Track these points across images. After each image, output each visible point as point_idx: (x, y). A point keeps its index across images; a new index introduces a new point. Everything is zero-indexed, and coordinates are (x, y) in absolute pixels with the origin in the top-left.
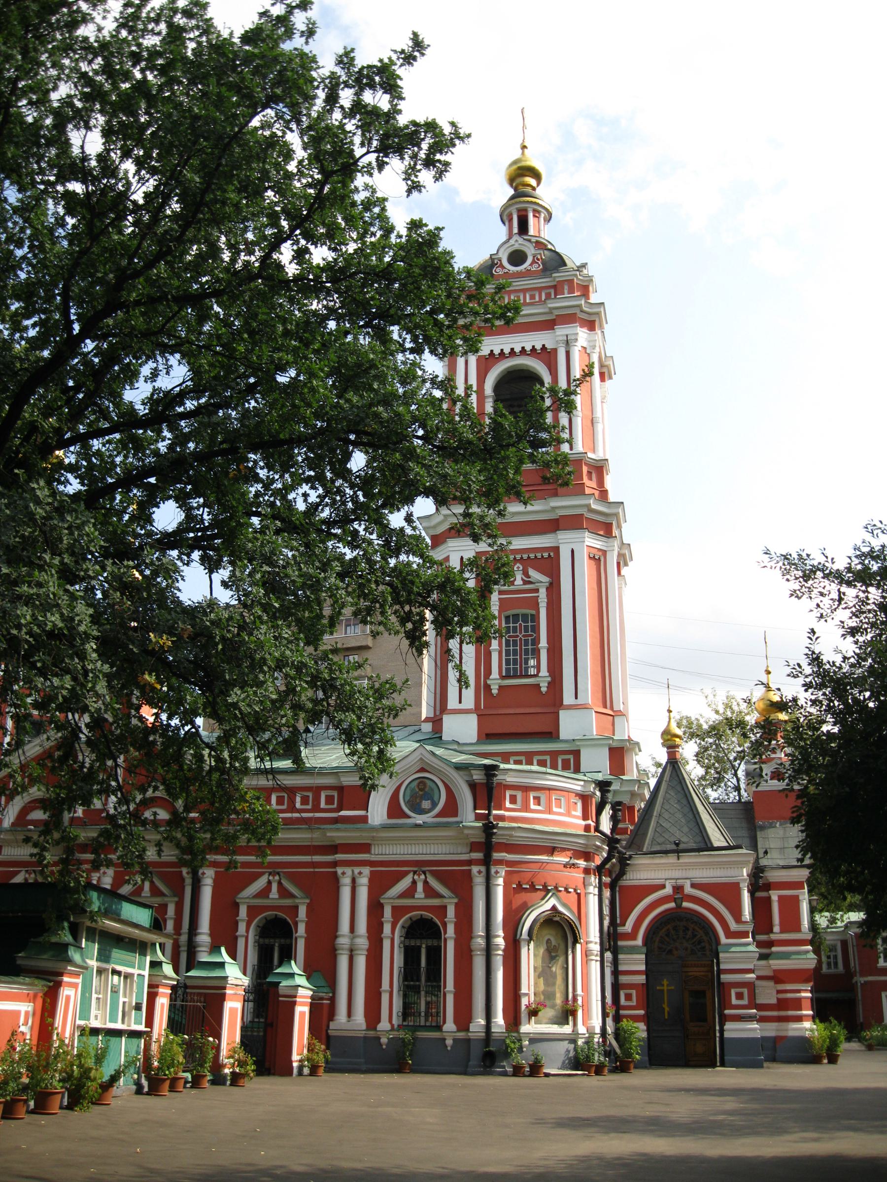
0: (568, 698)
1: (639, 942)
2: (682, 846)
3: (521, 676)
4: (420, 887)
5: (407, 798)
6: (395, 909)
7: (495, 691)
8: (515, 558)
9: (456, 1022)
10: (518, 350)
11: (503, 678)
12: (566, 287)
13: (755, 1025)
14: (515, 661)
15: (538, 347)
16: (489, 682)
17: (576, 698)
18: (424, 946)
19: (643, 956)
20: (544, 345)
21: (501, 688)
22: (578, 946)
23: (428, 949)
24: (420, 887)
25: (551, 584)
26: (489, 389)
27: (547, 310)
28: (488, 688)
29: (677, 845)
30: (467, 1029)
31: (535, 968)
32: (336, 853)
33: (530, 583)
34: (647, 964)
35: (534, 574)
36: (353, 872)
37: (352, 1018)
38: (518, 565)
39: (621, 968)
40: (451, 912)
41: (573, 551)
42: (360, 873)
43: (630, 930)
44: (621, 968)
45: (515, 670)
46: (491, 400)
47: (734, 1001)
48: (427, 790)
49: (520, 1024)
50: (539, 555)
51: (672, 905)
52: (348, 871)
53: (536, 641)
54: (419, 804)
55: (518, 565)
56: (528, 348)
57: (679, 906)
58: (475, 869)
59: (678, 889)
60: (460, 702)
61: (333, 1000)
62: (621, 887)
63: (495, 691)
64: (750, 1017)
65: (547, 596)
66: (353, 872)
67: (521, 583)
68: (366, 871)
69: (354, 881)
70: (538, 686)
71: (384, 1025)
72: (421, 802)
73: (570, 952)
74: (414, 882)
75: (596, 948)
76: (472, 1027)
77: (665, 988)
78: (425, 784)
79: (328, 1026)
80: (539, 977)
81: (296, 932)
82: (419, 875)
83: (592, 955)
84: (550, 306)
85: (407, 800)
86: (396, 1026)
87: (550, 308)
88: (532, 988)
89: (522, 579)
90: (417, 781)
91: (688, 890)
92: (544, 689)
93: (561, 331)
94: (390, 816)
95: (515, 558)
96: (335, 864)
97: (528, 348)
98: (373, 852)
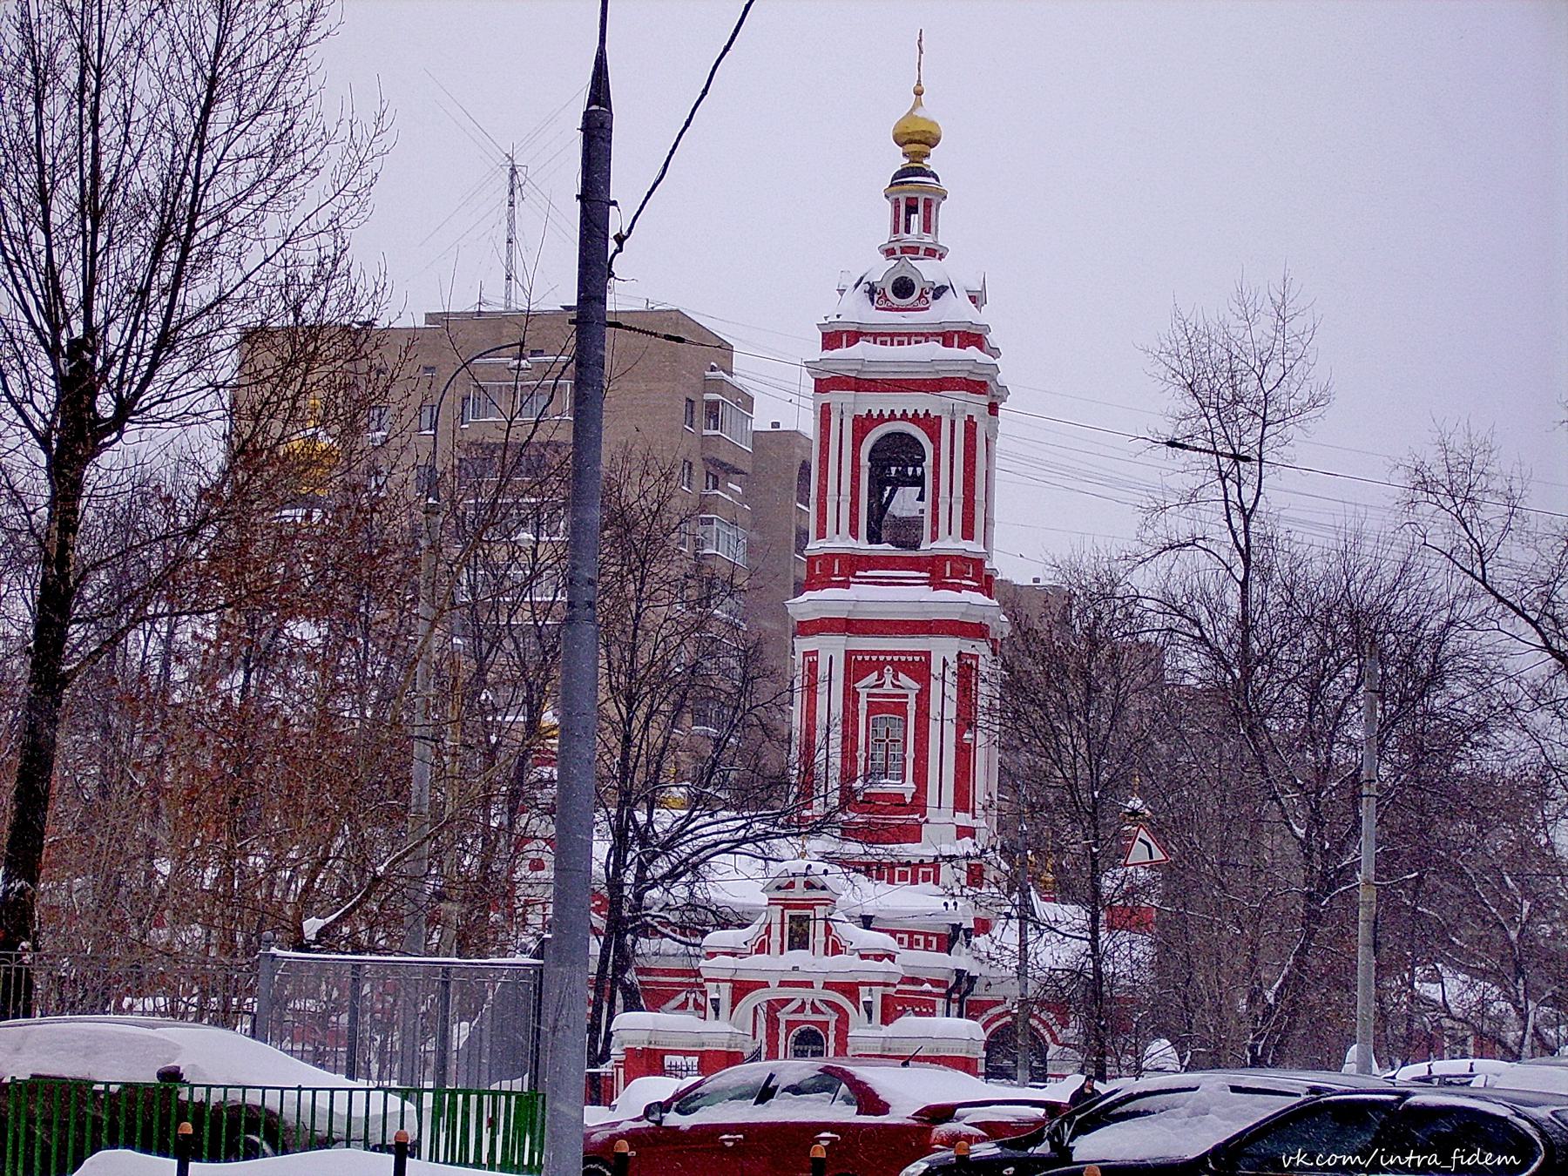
10: (898, 414)
25: (921, 690)
33: (899, 687)
55: (888, 667)
89: (892, 683)
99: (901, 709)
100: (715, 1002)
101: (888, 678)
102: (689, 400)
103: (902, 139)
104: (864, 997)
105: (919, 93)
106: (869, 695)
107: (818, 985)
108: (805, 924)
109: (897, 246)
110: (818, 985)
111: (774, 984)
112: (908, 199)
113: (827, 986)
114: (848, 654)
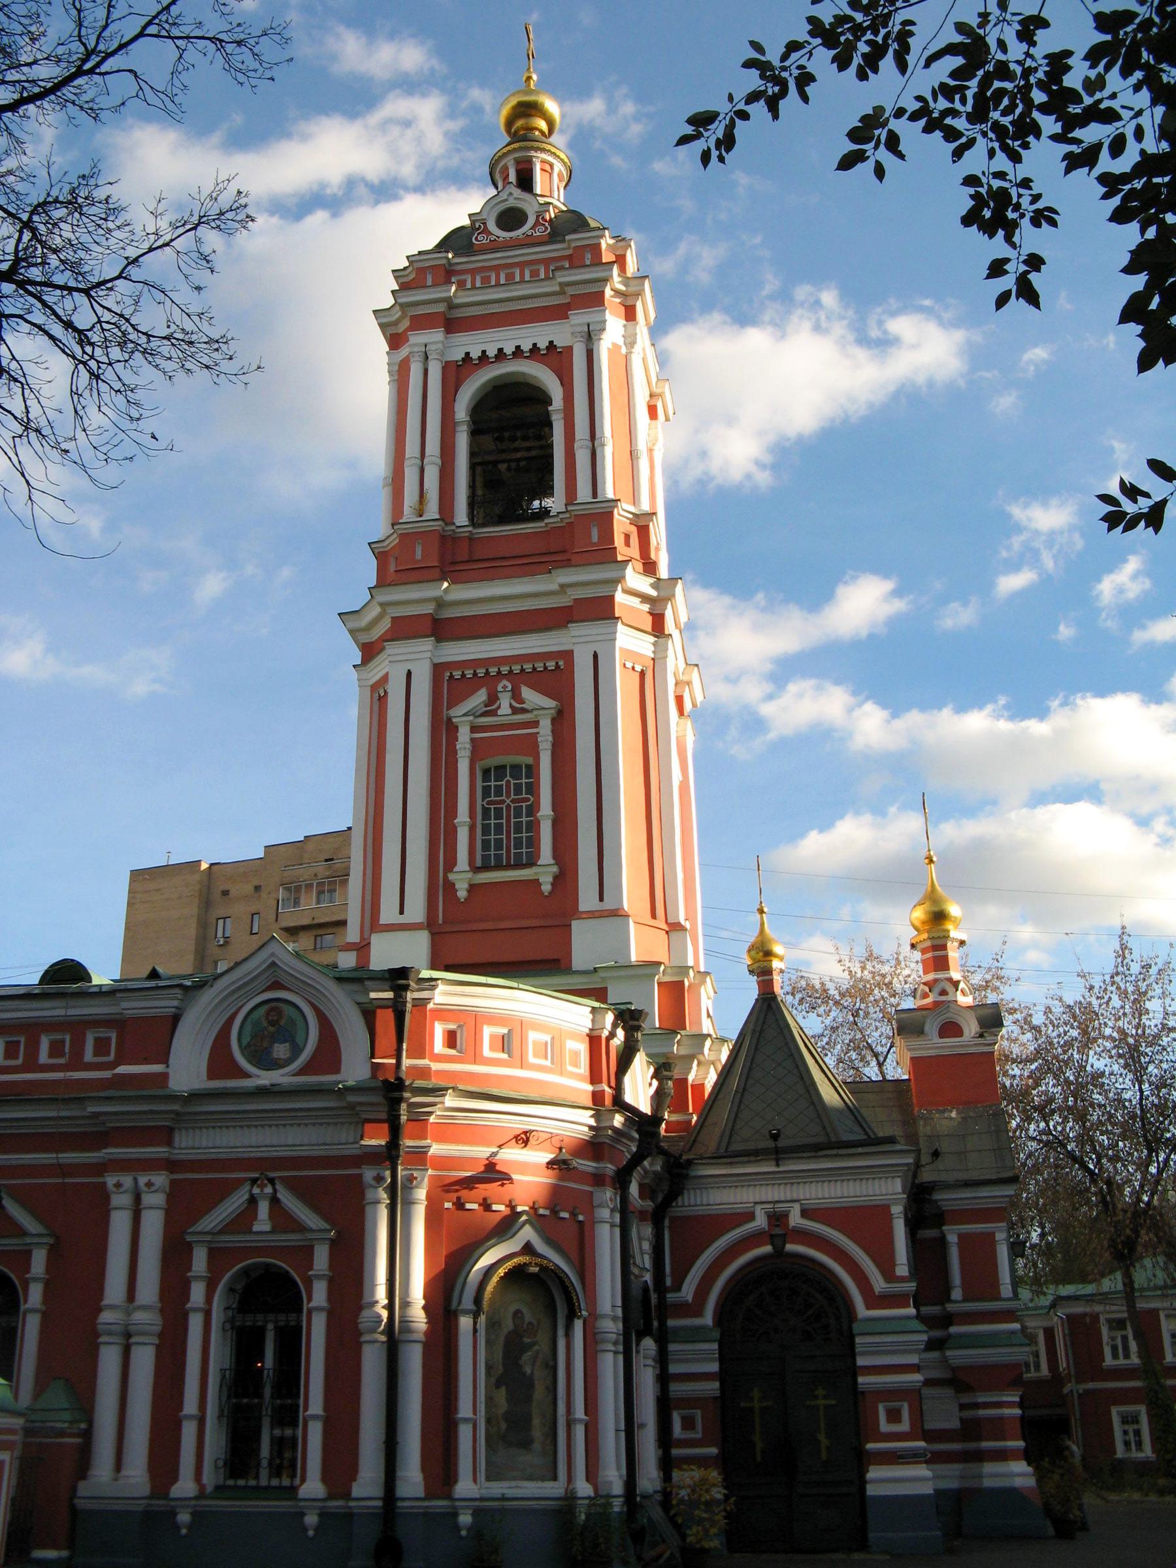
0: (587, 899)
1: (708, 1319)
2: (782, 1143)
3: (509, 867)
4: (263, 1208)
5: (246, 1040)
6: (215, 1254)
7: (462, 894)
8: (499, 672)
9: (326, 1478)
10: (509, 349)
11: (475, 869)
12: (588, 256)
13: (923, 1471)
14: (499, 843)
15: (543, 344)
16: (451, 877)
17: (601, 899)
18: (270, 1326)
19: (715, 1346)
20: (551, 342)
21: (472, 888)
22: (578, 1325)
23: (281, 1332)
24: (263, 1208)
25: (560, 712)
26: (461, 412)
27: (557, 288)
28: (450, 887)
29: (775, 1137)
30: (347, 1495)
31: (489, 1368)
32: (105, 1148)
33: (524, 711)
34: (722, 1360)
35: (530, 696)
36: (135, 1180)
37: (124, 1473)
39: (673, 1369)
40: (321, 1259)
41: (595, 656)
42: (149, 1184)
43: (690, 1298)
44: (673, 1369)
45: (498, 857)
46: (464, 428)
47: (885, 1427)
48: (282, 1022)
49: (456, 1481)
50: (540, 666)
51: (768, 1249)
52: (127, 1181)
53: (533, 810)
54: (268, 1051)
55: (505, 682)
56: (526, 347)
57: (779, 1253)
58: (369, 1174)
59: (778, 1218)
60: (402, 912)
61: (88, 1435)
62: (674, 1220)
63: (462, 894)
64: (915, 1455)
65: (553, 731)
66: (135, 1180)
67: (509, 711)
68: (161, 1179)
69: (138, 1198)
70: (536, 883)
71: (184, 1487)
72: (271, 1046)
73: (561, 1332)
74: (253, 1201)
75: (611, 1327)
76: (357, 1490)
77: (756, 1405)
78: (280, 1013)
79: (74, 1489)
80: (498, 1385)
81: (26, 1301)
82: (262, 1186)
83: (604, 1341)
84: (560, 280)
85: (245, 1042)
86: (209, 1489)
87: (562, 285)
88: (482, 1407)
89: (511, 706)
90: (266, 1007)
91: (795, 1219)
92: (546, 888)
93: (578, 318)
94: (212, 1074)
95: (499, 672)
96: (102, 1168)
97: (526, 347)
98: (176, 1144)
99: (531, 745)
106: (474, 729)
114: (438, 669)
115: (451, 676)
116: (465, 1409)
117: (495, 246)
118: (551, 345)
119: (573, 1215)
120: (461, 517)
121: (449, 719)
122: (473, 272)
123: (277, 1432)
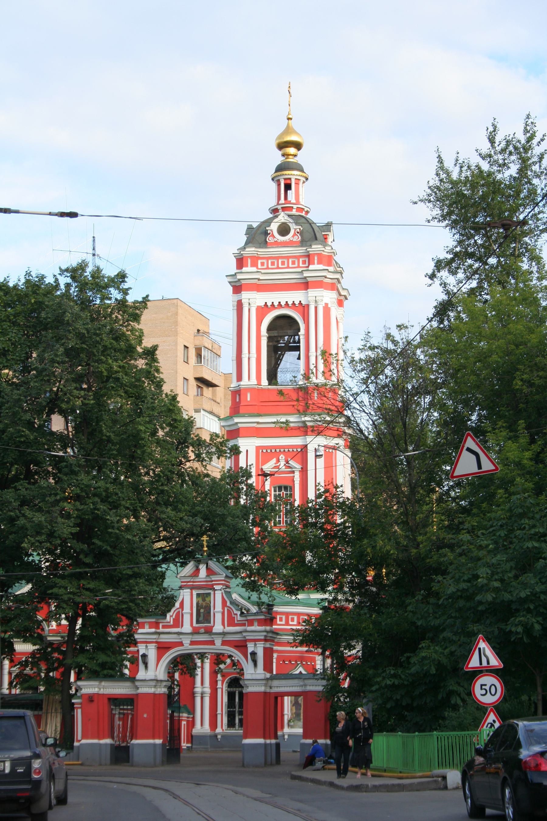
10: (283, 304)
12: (316, 258)
15: (297, 303)
18: (237, 692)
31: (291, 702)
33: (290, 467)
38: (282, 455)
56: (290, 303)
61: (193, 718)
67: (284, 468)
71: (219, 730)
93: (313, 293)
97: (290, 303)
100: (144, 656)
101: (282, 463)
102: (186, 347)
103: (282, 146)
104: (251, 648)
105: (289, 119)
107: (218, 642)
108: (207, 599)
109: (279, 207)
110: (218, 642)
111: (186, 641)
112: (285, 179)
113: (224, 643)
114: (258, 448)
115: (262, 451)
116: (286, 712)
117: (277, 244)
118: (300, 303)
119: (311, 663)
120: (265, 382)
121: (262, 469)
122: (268, 259)
123: (240, 717)
